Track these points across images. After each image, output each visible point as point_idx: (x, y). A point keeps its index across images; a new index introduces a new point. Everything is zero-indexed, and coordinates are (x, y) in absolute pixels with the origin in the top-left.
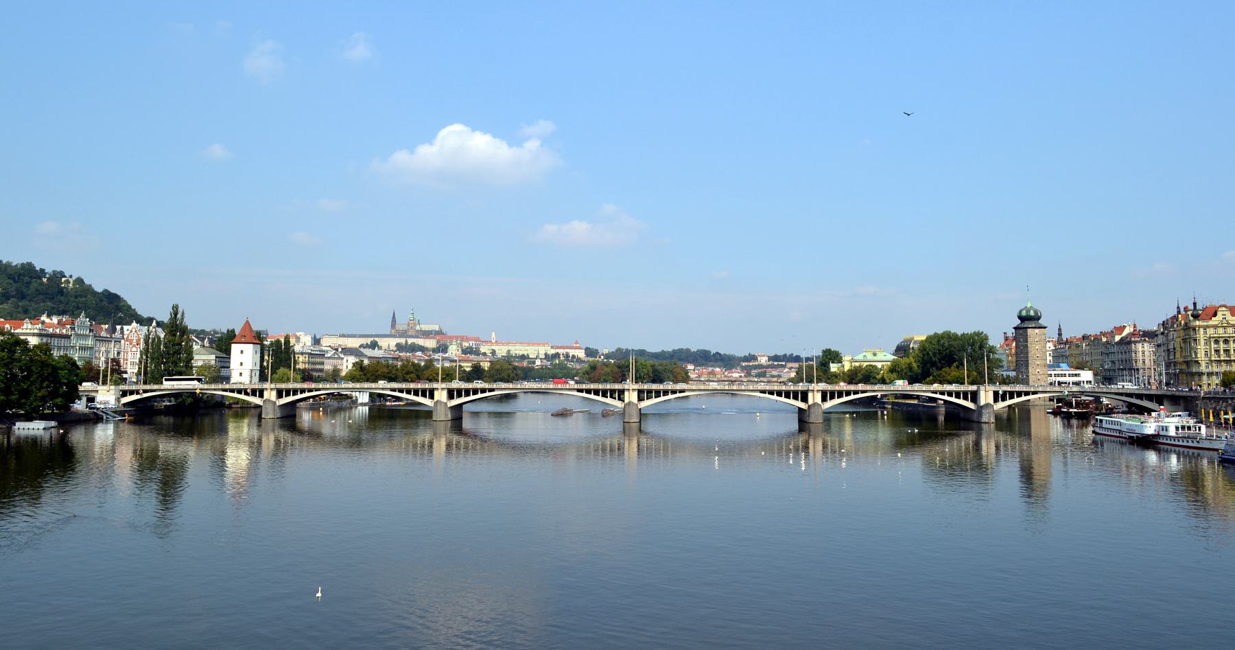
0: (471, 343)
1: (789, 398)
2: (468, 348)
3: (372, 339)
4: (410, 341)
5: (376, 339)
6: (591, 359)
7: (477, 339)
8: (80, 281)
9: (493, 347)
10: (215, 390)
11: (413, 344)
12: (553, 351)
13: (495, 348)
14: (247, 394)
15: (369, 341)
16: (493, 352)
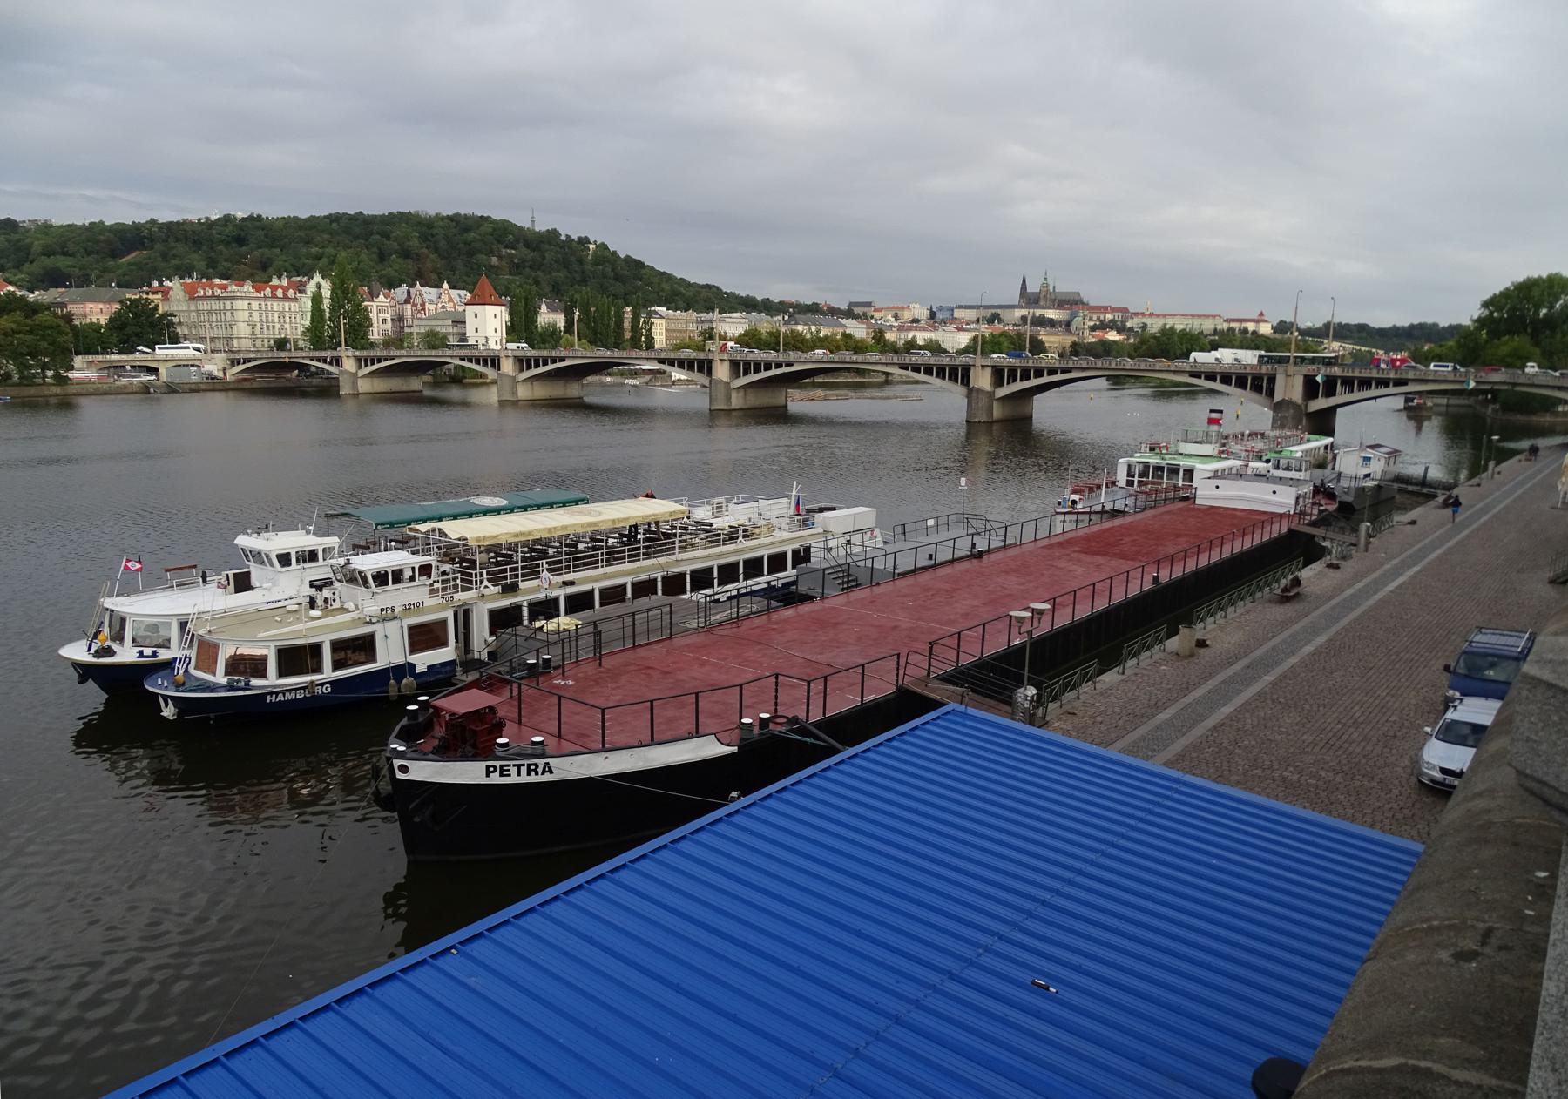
0: (1116, 314)
1: (944, 378)
2: (1112, 321)
3: (993, 311)
4: (1038, 312)
5: (998, 311)
6: (1278, 336)
7: (1125, 310)
8: (604, 247)
9: (1144, 320)
10: (303, 358)
11: (1042, 317)
12: (1225, 326)
13: (1148, 321)
14: (331, 364)
15: (989, 312)
16: (1144, 326)
